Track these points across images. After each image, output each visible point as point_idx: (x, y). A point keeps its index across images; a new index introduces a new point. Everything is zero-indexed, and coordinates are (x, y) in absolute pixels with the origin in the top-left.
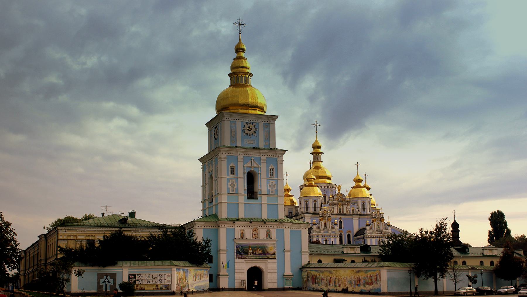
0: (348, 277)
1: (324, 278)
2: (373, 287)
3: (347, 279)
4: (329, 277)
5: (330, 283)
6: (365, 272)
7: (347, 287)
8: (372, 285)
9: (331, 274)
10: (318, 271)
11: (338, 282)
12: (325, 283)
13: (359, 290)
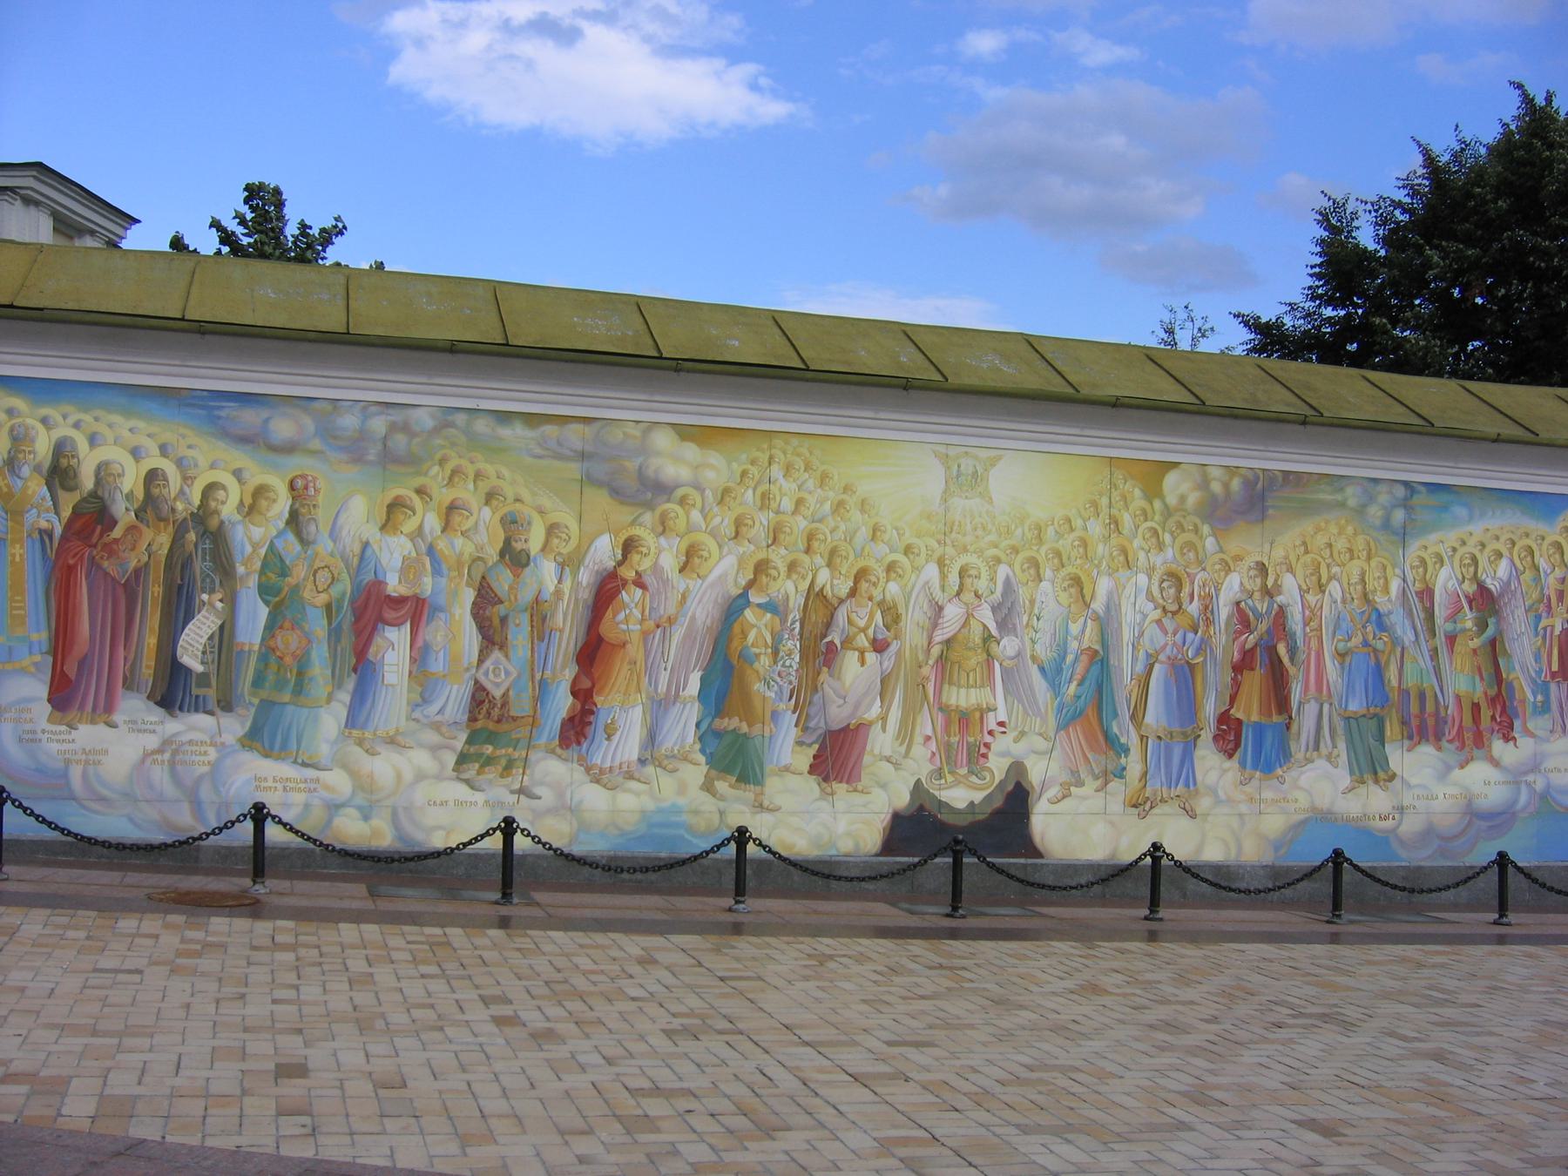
0: (1045, 585)
1: (427, 586)
2: (1516, 777)
3: (1005, 625)
4: (567, 564)
5: (584, 696)
6: (1386, 525)
7: (1018, 768)
8: (1498, 746)
9: (617, 493)
10: (250, 417)
11: (805, 696)
12: (453, 699)
13: (1274, 824)
